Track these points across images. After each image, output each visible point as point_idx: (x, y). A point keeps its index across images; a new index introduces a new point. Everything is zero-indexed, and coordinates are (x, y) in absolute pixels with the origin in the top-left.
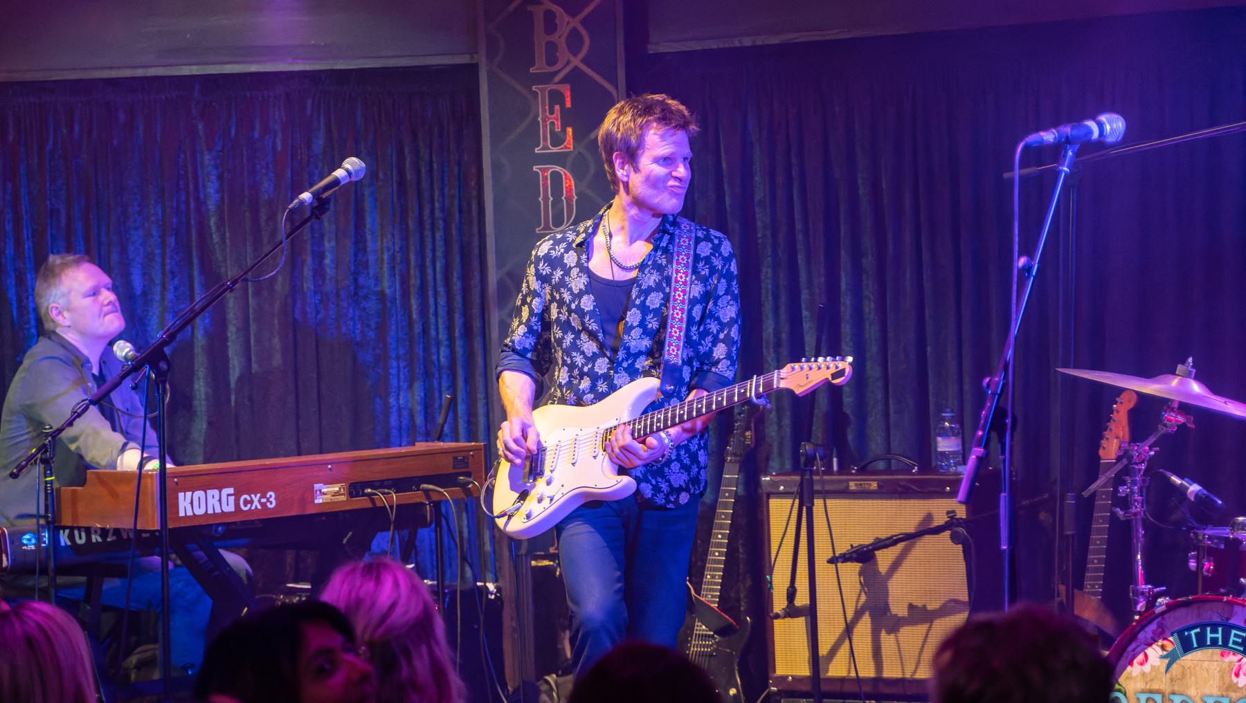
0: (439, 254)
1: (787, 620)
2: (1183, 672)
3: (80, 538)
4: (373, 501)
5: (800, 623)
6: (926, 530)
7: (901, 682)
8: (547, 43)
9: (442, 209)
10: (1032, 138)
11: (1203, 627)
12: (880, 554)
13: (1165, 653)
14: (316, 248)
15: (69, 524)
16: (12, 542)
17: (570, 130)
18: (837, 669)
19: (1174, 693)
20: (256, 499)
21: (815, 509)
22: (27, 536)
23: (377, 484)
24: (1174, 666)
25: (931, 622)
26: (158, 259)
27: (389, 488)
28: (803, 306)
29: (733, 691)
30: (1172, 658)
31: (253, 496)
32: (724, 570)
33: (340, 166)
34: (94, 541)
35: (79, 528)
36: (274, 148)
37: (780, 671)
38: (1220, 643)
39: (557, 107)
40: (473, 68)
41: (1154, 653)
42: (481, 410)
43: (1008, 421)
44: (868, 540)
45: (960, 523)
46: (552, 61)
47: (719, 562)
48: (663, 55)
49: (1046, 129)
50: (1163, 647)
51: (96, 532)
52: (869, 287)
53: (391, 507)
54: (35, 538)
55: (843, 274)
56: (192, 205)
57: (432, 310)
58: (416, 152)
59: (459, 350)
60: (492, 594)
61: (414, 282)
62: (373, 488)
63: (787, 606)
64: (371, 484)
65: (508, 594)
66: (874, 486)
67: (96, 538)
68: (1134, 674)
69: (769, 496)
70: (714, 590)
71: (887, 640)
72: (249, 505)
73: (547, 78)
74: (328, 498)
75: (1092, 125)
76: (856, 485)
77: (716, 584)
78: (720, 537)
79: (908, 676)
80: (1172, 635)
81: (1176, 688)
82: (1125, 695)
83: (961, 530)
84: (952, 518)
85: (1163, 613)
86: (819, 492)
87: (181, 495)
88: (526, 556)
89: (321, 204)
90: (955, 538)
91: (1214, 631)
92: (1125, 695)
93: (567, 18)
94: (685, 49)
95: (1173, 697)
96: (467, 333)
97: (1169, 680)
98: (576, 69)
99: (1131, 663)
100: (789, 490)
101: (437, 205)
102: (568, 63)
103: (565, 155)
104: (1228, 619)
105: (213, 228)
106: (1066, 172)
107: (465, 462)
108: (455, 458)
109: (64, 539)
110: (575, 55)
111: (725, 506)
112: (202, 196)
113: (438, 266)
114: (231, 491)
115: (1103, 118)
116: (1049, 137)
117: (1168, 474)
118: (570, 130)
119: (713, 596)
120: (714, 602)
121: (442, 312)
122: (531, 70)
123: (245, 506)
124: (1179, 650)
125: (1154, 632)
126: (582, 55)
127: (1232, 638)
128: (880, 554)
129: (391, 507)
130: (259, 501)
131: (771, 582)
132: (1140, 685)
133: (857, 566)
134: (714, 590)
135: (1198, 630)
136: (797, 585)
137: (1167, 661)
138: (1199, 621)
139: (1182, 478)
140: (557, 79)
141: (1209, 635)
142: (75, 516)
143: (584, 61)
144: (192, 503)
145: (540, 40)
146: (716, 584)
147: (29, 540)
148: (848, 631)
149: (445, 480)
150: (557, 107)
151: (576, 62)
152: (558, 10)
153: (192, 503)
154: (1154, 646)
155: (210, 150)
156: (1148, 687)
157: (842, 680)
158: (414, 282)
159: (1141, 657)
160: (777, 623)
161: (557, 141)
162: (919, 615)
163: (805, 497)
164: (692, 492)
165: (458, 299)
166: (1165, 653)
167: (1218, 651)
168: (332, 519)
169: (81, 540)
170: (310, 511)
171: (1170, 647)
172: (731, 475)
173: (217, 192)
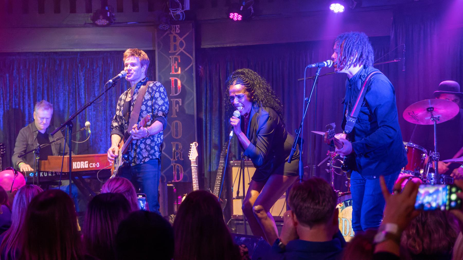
1: (237, 200)
2: (345, 212)
3: (46, 174)
10: (309, 66)
13: (341, 207)
14: (110, 99)
16: (27, 175)
17: (180, 68)
19: (343, 218)
20: (94, 164)
21: (245, 170)
22: (31, 174)
24: (343, 210)
26: (67, 101)
31: (93, 164)
33: (120, 73)
34: (49, 175)
35: (45, 172)
36: (99, 71)
43: (302, 141)
46: (175, 49)
47: (218, 184)
48: (205, 48)
49: (313, 64)
51: (50, 173)
54: (33, 174)
56: (77, 86)
63: (237, 196)
67: (50, 175)
69: (232, 166)
70: (217, 192)
72: (92, 166)
73: (174, 54)
75: (325, 62)
77: (218, 190)
78: (219, 178)
80: (342, 202)
81: (344, 217)
85: (340, 197)
86: (246, 166)
87: (74, 163)
88: (166, 182)
93: (179, 38)
94: (212, 47)
95: (343, 219)
97: (341, 214)
98: (182, 52)
102: (180, 50)
103: (178, 75)
105: (83, 93)
106: (318, 75)
111: (220, 169)
112: (79, 84)
114: (87, 162)
116: (314, 66)
117: (340, 160)
118: (180, 68)
119: (217, 194)
120: (217, 195)
124: (344, 205)
130: (95, 165)
131: (233, 189)
135: (349, 201)
136: (240, 190)
138: (350, 199)
140: (177, 54)
142: (45, 168)
143: (184, 50)
144: (76, 165)
145: (172, 44)
146: (218, 190)
147: (32, 175)
150: (176, 62)
151: (182, 50)
152: (176, 35)
153: (76, 165)
155: (82, 71)
160: (234, 201)
161: (176, 71)
166: (341, 207)
169: (46, 175)
171: (342, 206)
172: (222, 161)
173: (84, 83)
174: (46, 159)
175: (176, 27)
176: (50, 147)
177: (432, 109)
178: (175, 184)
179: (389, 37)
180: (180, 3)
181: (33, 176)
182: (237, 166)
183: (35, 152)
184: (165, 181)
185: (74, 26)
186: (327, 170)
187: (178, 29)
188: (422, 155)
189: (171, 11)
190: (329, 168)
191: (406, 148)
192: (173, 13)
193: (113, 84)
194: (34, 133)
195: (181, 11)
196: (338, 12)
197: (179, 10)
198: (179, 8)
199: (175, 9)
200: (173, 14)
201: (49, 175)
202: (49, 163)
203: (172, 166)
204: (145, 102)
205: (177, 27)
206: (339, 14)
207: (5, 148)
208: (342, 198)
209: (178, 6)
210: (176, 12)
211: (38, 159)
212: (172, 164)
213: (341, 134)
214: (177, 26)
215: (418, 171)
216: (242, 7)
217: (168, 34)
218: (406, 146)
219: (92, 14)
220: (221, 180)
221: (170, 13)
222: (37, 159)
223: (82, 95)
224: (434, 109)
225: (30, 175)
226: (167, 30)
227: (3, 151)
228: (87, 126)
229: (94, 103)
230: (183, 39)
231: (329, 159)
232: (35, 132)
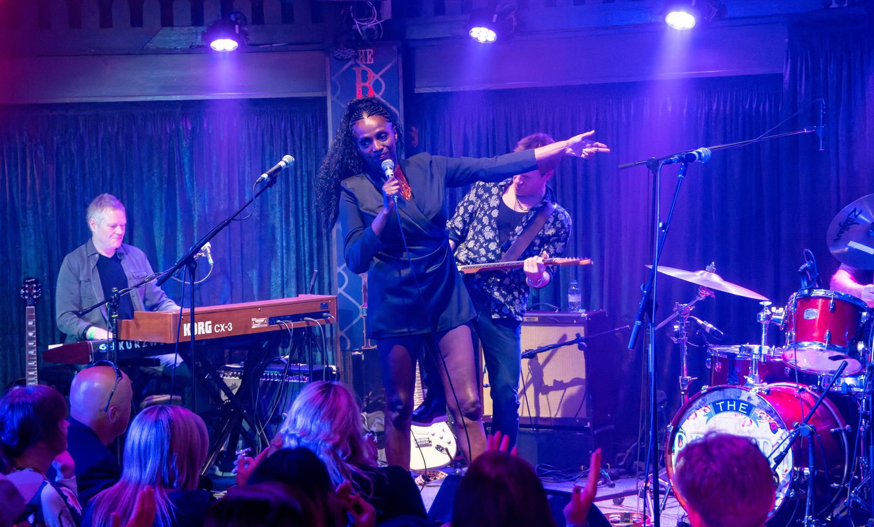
0: (305, 194)
3: (129, 346)
4: (281, 326)
6: (563, 342)
7: (550, 419)
9: (307, 172)
11: (726, 401)
12: (538, 354)
13: (706, 414)
15: (125, 339)
16: (94, 349)
22: (103, 345)
24: (711, 420)
25: (565, 390)
27: (288, 319)
30: (710, 416)
33: (281, 160)
34: (136, 347)
38: (735, 409)
40: (323, 100)
41: (700, 413)
42: (326, 276)
44: (535, 348)
53: (291, 330)
57: (301, 223)
58: (294, 142)
59: (315, 244)
60: (334, 371)
61: (292, 208)
62: (281, 320)
64: (279, 318)
65: (342, 370)
66: (537, 319)
67: (137, 346)
74: (258, 326)
76: (527, 319)
79: (553, 416)
80: (709, 404)
83: (584, 343)
85: (705, 394)
87: (185, 325)
89: (273, 177)
90: (580, 348)
91: (732, 403)
93: (373, 74)
94: (434, 91)
96: (319, 234)
99: (688, 418)
104: (739, 397)
105: (188, 180)
107: (326, 306)
108: (322, 304)
109: (121, 347)
114: (210, 322)
115: (700, 150)
117: (696, 318)
121: (306, 224)
124: (713, 412)
125: (700, 403)
126: (381, 93)
127: (741, 407)
128: (538, 354)
129: (291, 330)
130: (224, 327)
132: (693, 430)
133: (527, 360)
135: (723, 402)
137: (707, 418)
139: (703, 321)
141: (729, 405)
147: (103, 347)
156: (697, 431)
158: (292, 208)
159: (693, 415)
160: (484, 389)
166: (706, 414)
167: (733, 413)
168: (259, 336)
169: (129, 348)
170: (249, 332)
171: (708, 411)
178: (365, 352)
179: (781, 76)
180: (374, 7)
181: (106, 350)
183: (108, 304)
184: (348, 347)
185: (171, 52)
186: (675, 339)
187: (369, 56)
188: (861, 314)
189: (356, 22)
190: (677, 334)
191: (831, 301)
192: (361, 26)
193: (269, 182)
195: (375, 22)
197: (373, 20)
198: (371, 16)
200: (360, 27)
201: (136, 347)
202: (138, 325)
203: (362, 319)
205: (368, 53)
207: (40, 287)
208: (707, 397)
209: (370, 14)
211: (116, 317)
212: (361, 316)
213: (702, 272)
216: (495, 16)
217: (351, 66)
218: (830, 299)
221: (354, 27)
222: (113, 318)
223: (186, 183)
225: (101, 348)
226: (348, 60)
229: (235, 220)
230: (380, 76)
231: (678, 318)
232: (93, 256)
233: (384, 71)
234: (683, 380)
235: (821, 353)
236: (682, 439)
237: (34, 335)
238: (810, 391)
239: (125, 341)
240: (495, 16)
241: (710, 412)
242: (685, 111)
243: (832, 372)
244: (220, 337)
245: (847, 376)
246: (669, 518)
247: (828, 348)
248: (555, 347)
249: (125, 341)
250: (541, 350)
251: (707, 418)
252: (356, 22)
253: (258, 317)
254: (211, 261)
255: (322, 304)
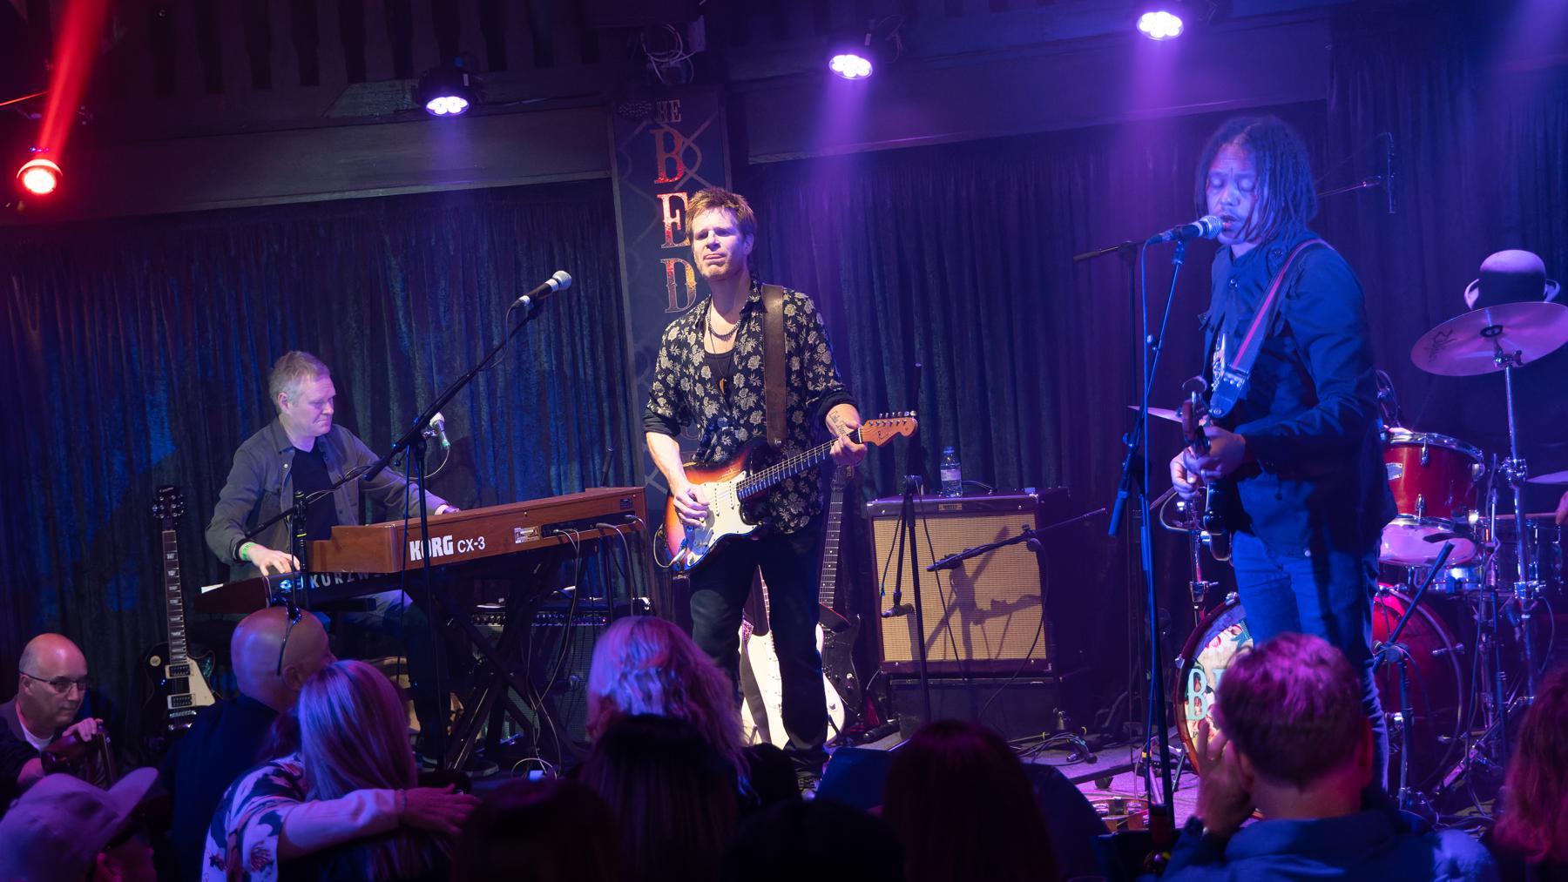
3: (326, 581)
4: (560, 538)
5: (902, 621)
6: (1003, 541)
7: (987, 662)
8: (667, 159)
12: (965, 561)
13: (1235, 637)
15: (319, 571)
16: (273, 588)
18: (934, 655)
22: (285, 582)
23: (561, 525)
28: (884, 362)
29: (849, 676)
32: (836, 579)
34: (337, 582)
37: (888, 657)
39: (678, 212)
40: (609, 180)
44: (959, 552)
45: (1032, 535)
46: (671, 174)
47: (831, 572)
48: (760, 165)
50: (1233, 632)
51: (338, 575)
52: (938, 347)
53: (576, 543)
54: (291, 583)
55: (916, 335)
63: (895, 607)
64: (556, 526)
65: (658, 603)
66: (959, 507)
67: (338, 581)
68: (1210, 655)
69: (873, 520)
70: (829, 595)
71: (975, 630)
73: (667, 188)
75: (1196, 224)
77: (830, 590)
79: (993, 657)
80: (1240, 622)
82: (1203, 671)
84: (1026, 530)
85: (1232, 606)
87: (412, 543)
90: (1031, 547)
92: (1203, 671)
93: (682, 139)
98: (692, 179)
99: (1207, 646)
100: (888, 513)
101: (582, 294)
102: (686, 173)
107: (629, 504)
108: (622, 500)
109: (314, 583)
110: (690, 169)
113: (585, 342)
114: (450, 537)
120: (831, 605)
122: (655, 182)
123: (462, 549)
128: (965, 561)
130: (472, 544)
134: (829, 595)
137: (1236, 643)
140: (676, 188)
142: (323, 564)
143: (698, 173)
145: (661, 156)
146: (830, 590)
147: (286, 585)
148: (944, 622)
149: (617, 519)
150: (678, 212)
151: (691, 173)
152: (675, 132)
154: (1225, 631)
157: (940, 663)
159: (1215, 640)
162: (1000, 608)
163: (908, 517)
164: (812, 514)
165: (603, 368)
166: (1235, 637)
170: (512, 550)
171: (1238, 632)
174: (328, 535)
175: (669, 105)
176: (330, 499)
177: (1497, 331)
181: (291, 589)
182: (887, 517)
188: (1471, 468)
191: (1424, 449)
192: (659, 65)
194: (283, 453)
195: (681, 56)
196: (1163, 38)
199: (663, 53)
200: (657, 67)
202: (338, 549)
204: (741, 417)
205: (672, 105)
206: (1167, 42)
207: (182, 499)
208: (1236, 610)
210: (666, 60)
214: (672, 102)
215: (1464, 517)
216: (869, 35)
219: (415, 83)
220: (839, 559)
223: (400, 325)
224: (1504, 329)
225: (283, 587)
227: (177, 508)
228: (436, 428)
233: (696, 135)
234: (1195, 587)
235: (1411, 532)
236: (1200, 679)
237: (176, 574)
238: (1396, 593)
239: (319, 574)
240: (869, 35)
241: (1242, 635)
242: (1175, 168)
243: (1429, 561)
244: (468, 558)
245: (1453, 567)
246: (1185, 805)
247: (1423, 524)
248: (990, 548)
249: (319, 574)
250: (969, 554)
251: (1236, 643)
252: (652, 58)
253: (524, 527)
254: (446, 442)
255: (622, 500)
